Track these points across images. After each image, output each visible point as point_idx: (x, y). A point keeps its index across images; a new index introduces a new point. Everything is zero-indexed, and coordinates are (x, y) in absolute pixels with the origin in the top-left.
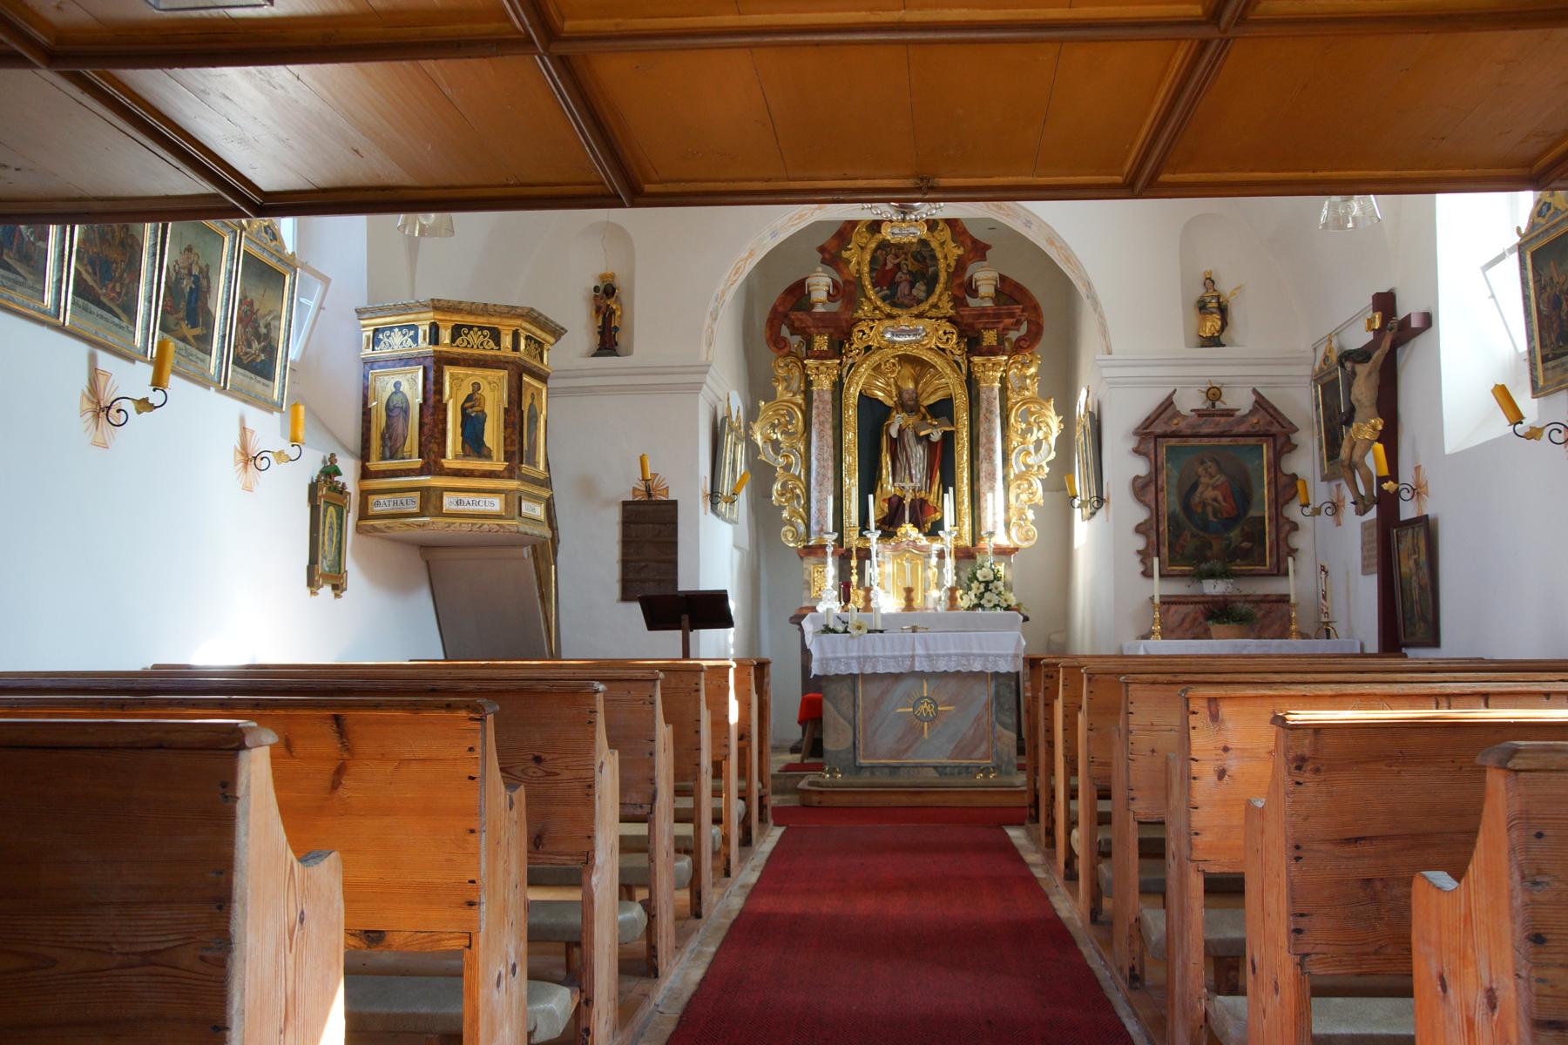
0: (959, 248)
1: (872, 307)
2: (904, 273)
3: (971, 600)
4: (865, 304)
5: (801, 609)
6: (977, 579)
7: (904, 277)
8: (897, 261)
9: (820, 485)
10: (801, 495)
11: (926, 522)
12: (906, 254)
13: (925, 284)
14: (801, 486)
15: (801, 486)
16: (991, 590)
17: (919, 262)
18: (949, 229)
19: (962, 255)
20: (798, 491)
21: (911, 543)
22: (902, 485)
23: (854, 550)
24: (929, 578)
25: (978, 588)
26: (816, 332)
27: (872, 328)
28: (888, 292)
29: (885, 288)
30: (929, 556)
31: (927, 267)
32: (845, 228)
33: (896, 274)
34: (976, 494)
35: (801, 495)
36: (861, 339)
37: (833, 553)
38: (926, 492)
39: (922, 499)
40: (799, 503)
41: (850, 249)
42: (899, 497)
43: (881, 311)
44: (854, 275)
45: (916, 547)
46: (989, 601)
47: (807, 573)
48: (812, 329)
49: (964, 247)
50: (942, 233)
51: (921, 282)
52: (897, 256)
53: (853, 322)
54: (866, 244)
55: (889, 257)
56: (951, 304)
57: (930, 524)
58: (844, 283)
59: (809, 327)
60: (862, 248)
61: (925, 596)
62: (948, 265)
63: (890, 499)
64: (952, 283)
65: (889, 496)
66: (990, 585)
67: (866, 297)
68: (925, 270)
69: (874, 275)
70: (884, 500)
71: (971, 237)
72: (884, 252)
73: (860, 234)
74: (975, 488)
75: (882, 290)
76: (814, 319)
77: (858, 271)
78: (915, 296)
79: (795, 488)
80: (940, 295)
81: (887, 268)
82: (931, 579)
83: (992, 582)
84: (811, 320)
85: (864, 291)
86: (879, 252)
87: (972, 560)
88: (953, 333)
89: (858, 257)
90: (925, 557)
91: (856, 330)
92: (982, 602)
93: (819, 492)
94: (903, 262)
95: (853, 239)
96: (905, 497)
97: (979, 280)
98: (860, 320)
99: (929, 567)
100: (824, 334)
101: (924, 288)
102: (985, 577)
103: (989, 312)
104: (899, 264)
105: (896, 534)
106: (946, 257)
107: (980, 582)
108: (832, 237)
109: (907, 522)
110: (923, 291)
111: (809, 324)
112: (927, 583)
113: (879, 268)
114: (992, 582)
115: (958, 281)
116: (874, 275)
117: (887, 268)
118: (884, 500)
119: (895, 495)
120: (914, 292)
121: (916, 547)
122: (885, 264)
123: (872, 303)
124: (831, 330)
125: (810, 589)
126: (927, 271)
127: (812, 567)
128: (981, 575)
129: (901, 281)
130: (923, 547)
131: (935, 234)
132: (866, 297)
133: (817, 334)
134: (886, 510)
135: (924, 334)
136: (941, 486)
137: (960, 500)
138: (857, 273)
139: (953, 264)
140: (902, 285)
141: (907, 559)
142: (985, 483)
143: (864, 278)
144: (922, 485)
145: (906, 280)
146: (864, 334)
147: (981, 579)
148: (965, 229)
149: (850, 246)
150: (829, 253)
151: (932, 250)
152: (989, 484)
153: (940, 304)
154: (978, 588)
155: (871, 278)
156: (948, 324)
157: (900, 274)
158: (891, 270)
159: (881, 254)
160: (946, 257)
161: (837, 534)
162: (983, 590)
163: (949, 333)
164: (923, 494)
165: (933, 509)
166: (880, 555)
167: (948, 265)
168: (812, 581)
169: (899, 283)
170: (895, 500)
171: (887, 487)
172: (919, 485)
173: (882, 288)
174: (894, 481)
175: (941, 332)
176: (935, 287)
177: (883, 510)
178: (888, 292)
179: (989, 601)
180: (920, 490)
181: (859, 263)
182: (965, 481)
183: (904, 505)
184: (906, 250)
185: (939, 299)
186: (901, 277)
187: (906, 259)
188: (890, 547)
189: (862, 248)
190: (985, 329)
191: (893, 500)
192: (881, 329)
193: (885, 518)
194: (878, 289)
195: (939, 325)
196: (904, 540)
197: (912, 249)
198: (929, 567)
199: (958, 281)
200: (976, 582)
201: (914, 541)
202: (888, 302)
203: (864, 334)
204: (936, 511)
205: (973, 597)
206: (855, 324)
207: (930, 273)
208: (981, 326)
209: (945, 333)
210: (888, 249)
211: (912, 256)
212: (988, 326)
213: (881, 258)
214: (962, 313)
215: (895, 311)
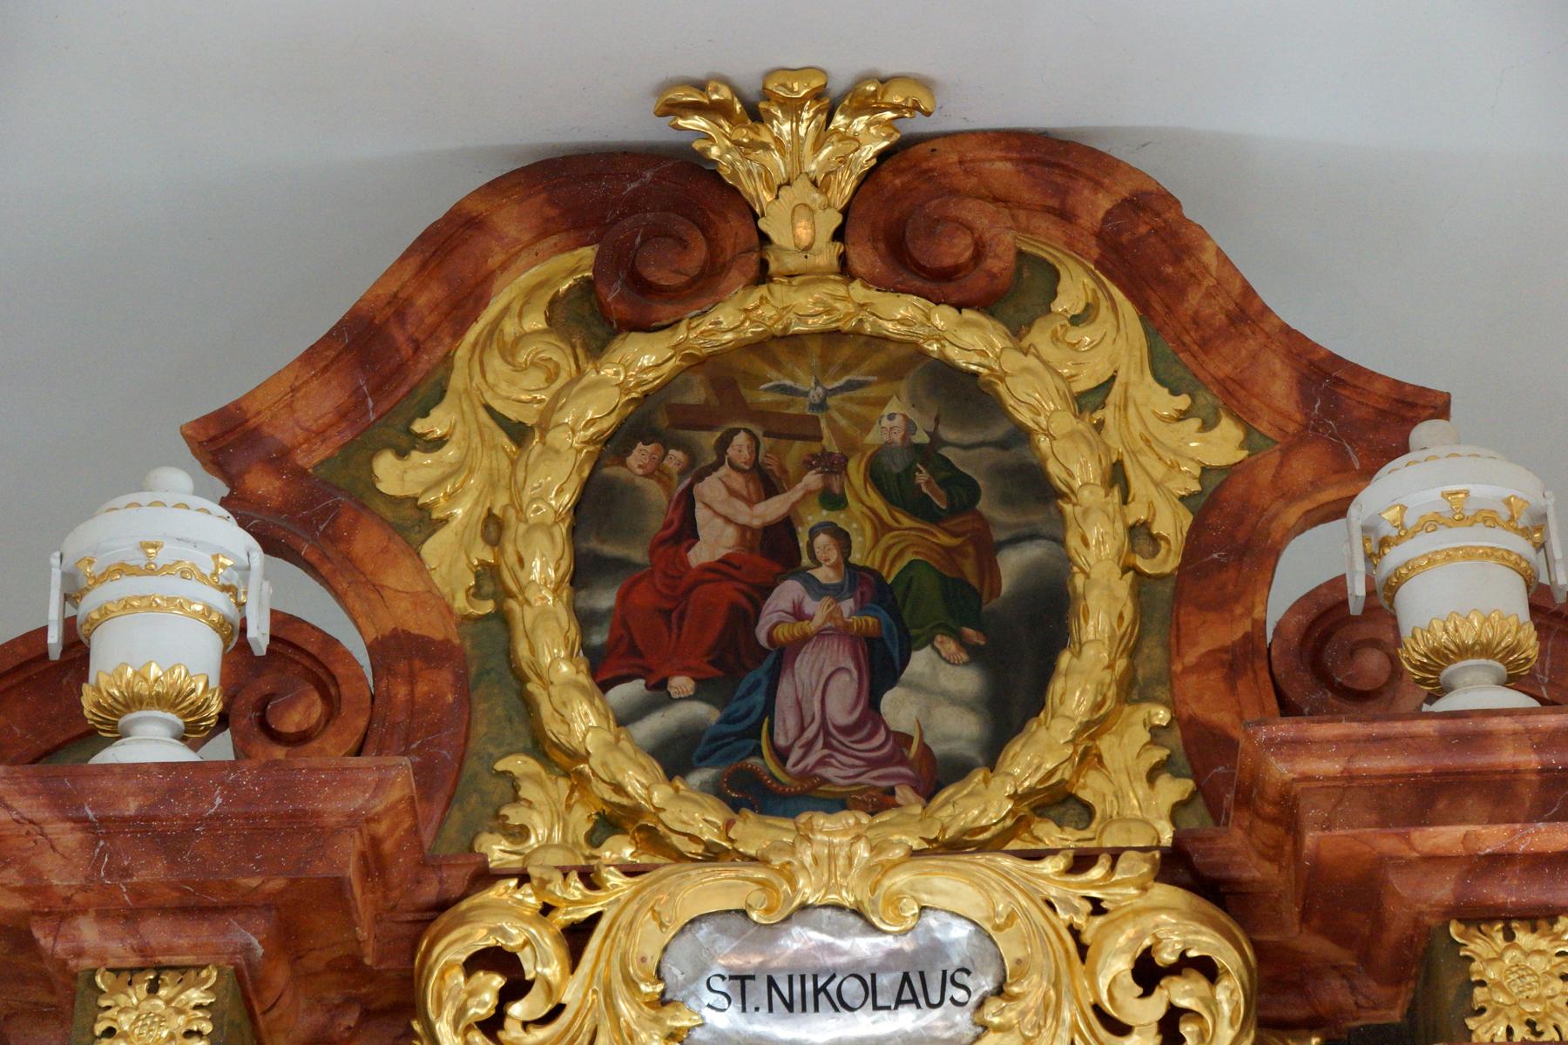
0: (1206, 426)
1: (581, 820)
2: (817, 589)
4: (528, 791)
7: (818, 610)
8: (772, 509)
12: (833, 465)
13: (976, 655)
17: (920, 508)
18: (1127, 308)
19: (1231, 471)
26: (119, 949)
27: (576, 937)
28: (702, 712)
29: (681, 684)
31: (987, 550)
32: (399, 306)
33: (766, 591)
36: (492, 1025)
41: (440, 443)
43: (653, 839)
44: (461, 603)
48: (88, 932)
49: (1244, 419)
50: (1073, 335)
51: (949, 647)
52: (767, 483)
53: (429, 892)
54: (552, 407)
55: (711, 489)
56: (1173, 789)
58: (371, 649)
59: (61, 914)
60: (519, 433)
62: (1140, 534)
64: (1173, 649)
67: (541, 747)
68: (969, 568)
69: (605, 600)
71: (1296, 346)
72: (676, 457)
73: (508, 353)
75: (660, 695)
76: (103, 829)
77: (489, 579)
78: (903, 740)
80: (1095, 727)
81: (701, 555)
84: (67, 837)
85: (528, 706)
86: (640, 455)
88: (1208, 969)
89: (492, 484)
91: (451, 950)
94: (816, 515)
95: (457, 381)
97: (1405, 533)
98: (486, 877)
100: (185, 973)
101: (967, 680)
103: (1508, 757)
104: (784, 528)
106: (1117, 477)
108: (309, 356)
110: (955, 700)
111: (61, 876)
113: (638, 554)
115: (1214, 635)
116: (605, 600)
117: (701, 555)
120: (899, 709)
122: (686, 531)
123: (580, 782)
124: (250, 937)
126: (989, 569)
129: (805, 639)
131: (1039, 337)
132: (541, 747)
133: (126, 974)
135: (987, 984)
138: (477, 593)
139: (1172, 524)
140: (805, 670)
143: (523, 616)
145: (840, 632)
146: (516, 988)
148: (1248, 291)
149: (434, 424)
150: (280, 460)
151: (1022, 435)
153: (1091, 788)
155: (586, 619)
156: (1163, 893)
157: (788, 592)
158: (722, 569)
159: (656, 472)
160: (1117, 477)
163: (1183, 965)
167: (1140, 534)
169: (782, 656)
173: (659, 686)
175: (1116, 966)
176: (1045, 672)
178: (702, 712)
181: (493, 527)
184: (830, 443)
185: (1089, 758)
186: (798, 614)
187: (833, 500)
189: (519, 433)
190: (1478, 916)
192: (648, 941)
194: (630, 691)
195: (1097, 908)
197: (874, 438)
199: (1214, 635)
202: (697, 778)
203: (516, 988)
206: (443, 906)
207: (1006, 584)
208: (1442, 890)
209: (1148, 973)
210: (707, 440)
211: (875, 476)
212: (1505, 892)
213: (655, 493)
214: (1281, 770)
215: (754, 833)
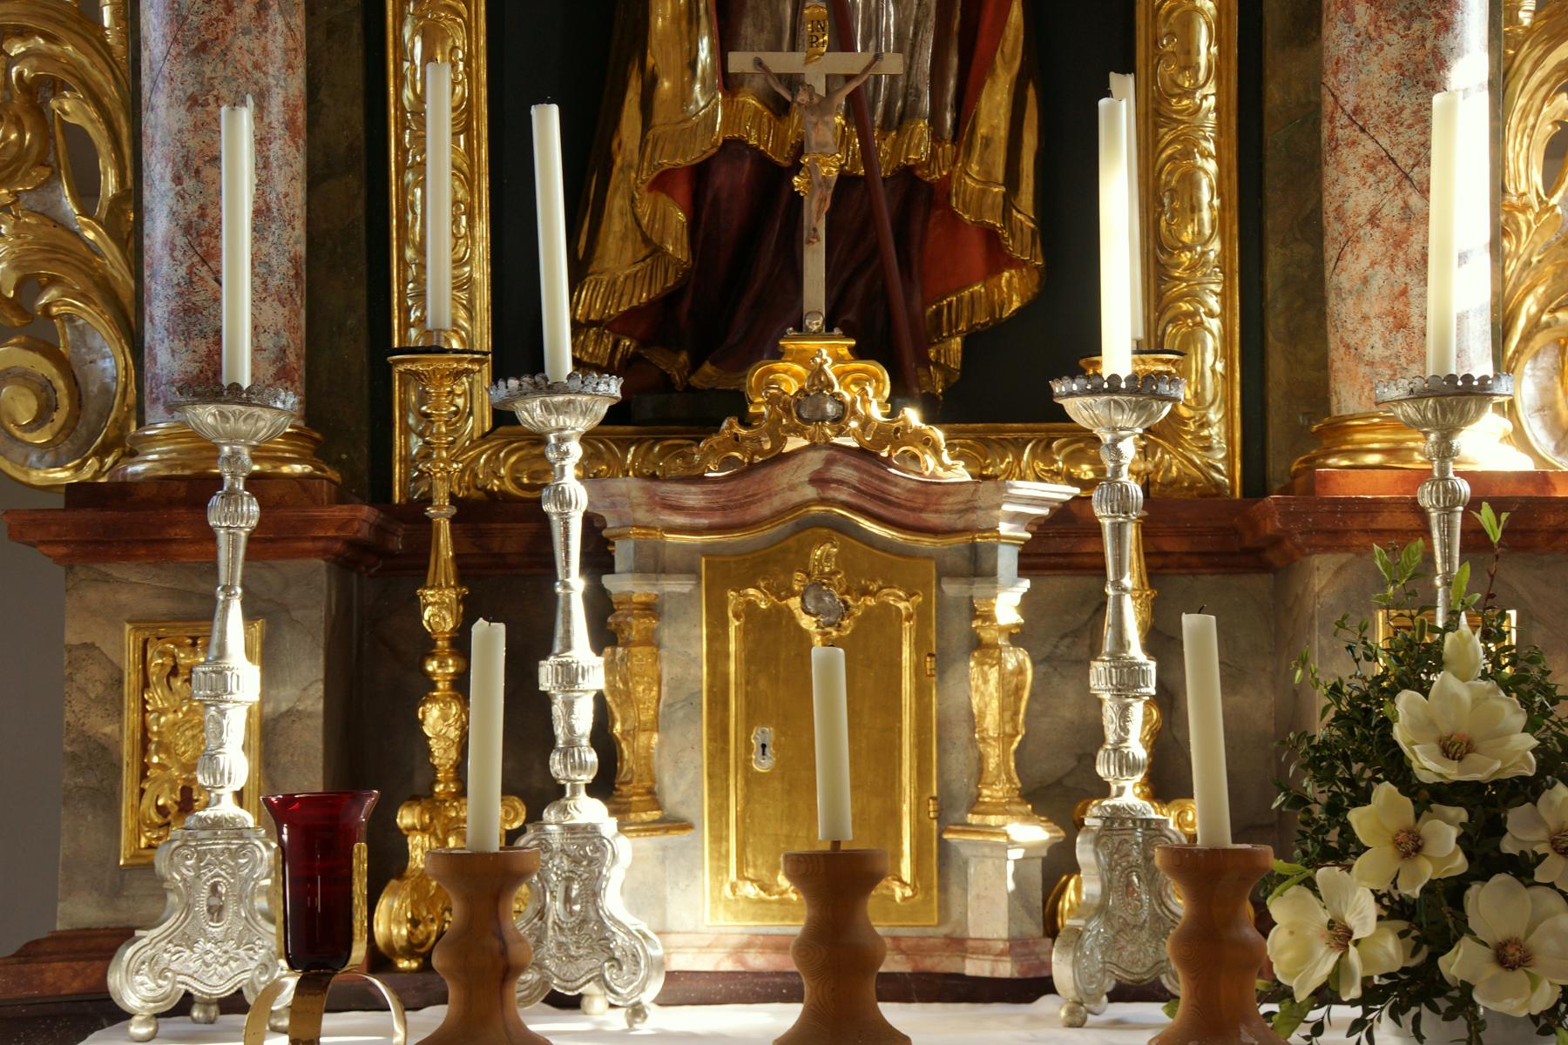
3: (1341, 935)
5: (31, 952)
6: (1397, 768)
9: (203, 48)
10: (98, 135)
11: (935, 331)
14: (99, 76)
15: (99, 76)
16: (1522, 868)
20: (70, 107)
21: (841, 471)
22: (784, 62)
23: (441, 514)
24: (972, 720)
25: (1411, 846)
30: (978, 566)
34: (1274, 136)
35: (98, 135)
37: (260, 545)
38: (937, 136)
39: (907, 175)
40: (86, 192)
42: (760, 158)
45: (879, 504)
46: (1511, 956)
47: (92, 677)
57: (956, 343)
61: (944, 848)
63: (700, 173)
65: (694, 156)
66: (1515, 817)
70: (662, 182)
74: (1274, 94)
79: (56, 87)
82: (991, 722)
83: (1524, 790)
87: (1259, 583)
90: (945, 573)
92: (1454, 965)
93: (193, 102)
96: (800, 150)
99: (977, 644)
102: (1452, 749)
105: (737, 405)
107: (1429, 797)
109: (815, 323)
112: (959, 761)
114: (1524, 790)
118: (662, 182)
119: (733, 147)
121: (879, 504)
125: (108, 801)
127: (130, 639)
128: (1424, 726)
130: (932, 492)
134: (676, 248)
136: (1031, 93)
137: (1170, 178)
141: (816, 586)
142: (1367, 39)
144: (911, 94)
147: (1427, 765)
152: (1395, 46)
154: (1411, 846)
161: (289, 400)
162: (1460, 864)
164: (919, 145)
165: (976, 252)
166: (622, 553)
168: (127, 750)
170: (731, 181)
171: (684, 96)
172: (893, 64)
174: (724, 47)
177: (655, 251)
179: (1511, 956)
180: (898, 122)
182: (1205, 49)
183: (797, 201)
188: (693, 496)
191: (721, 179)
193: (667, 303)
196: (794, 443)
198: (977, 644)
200: (1384, 792)
201: (864, 454)
204: (997, 257)
205: (1363, 915)
